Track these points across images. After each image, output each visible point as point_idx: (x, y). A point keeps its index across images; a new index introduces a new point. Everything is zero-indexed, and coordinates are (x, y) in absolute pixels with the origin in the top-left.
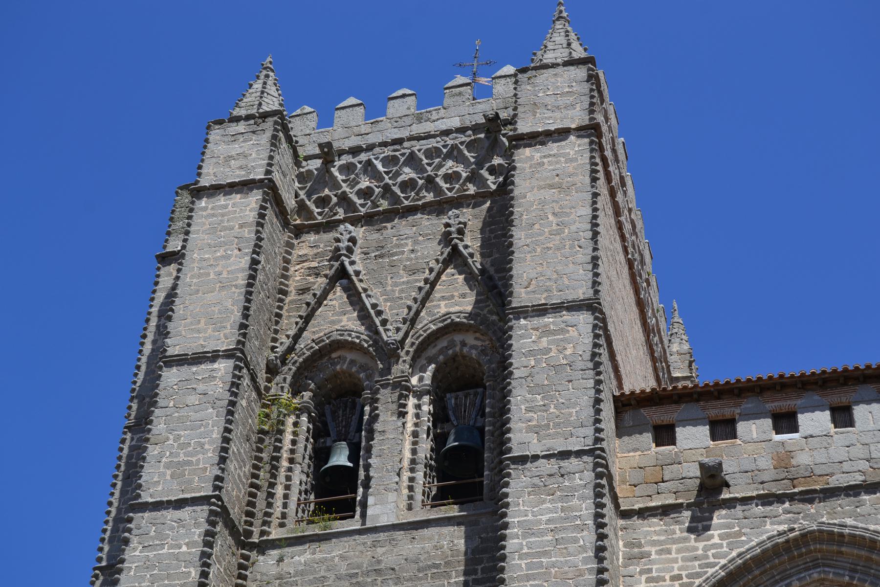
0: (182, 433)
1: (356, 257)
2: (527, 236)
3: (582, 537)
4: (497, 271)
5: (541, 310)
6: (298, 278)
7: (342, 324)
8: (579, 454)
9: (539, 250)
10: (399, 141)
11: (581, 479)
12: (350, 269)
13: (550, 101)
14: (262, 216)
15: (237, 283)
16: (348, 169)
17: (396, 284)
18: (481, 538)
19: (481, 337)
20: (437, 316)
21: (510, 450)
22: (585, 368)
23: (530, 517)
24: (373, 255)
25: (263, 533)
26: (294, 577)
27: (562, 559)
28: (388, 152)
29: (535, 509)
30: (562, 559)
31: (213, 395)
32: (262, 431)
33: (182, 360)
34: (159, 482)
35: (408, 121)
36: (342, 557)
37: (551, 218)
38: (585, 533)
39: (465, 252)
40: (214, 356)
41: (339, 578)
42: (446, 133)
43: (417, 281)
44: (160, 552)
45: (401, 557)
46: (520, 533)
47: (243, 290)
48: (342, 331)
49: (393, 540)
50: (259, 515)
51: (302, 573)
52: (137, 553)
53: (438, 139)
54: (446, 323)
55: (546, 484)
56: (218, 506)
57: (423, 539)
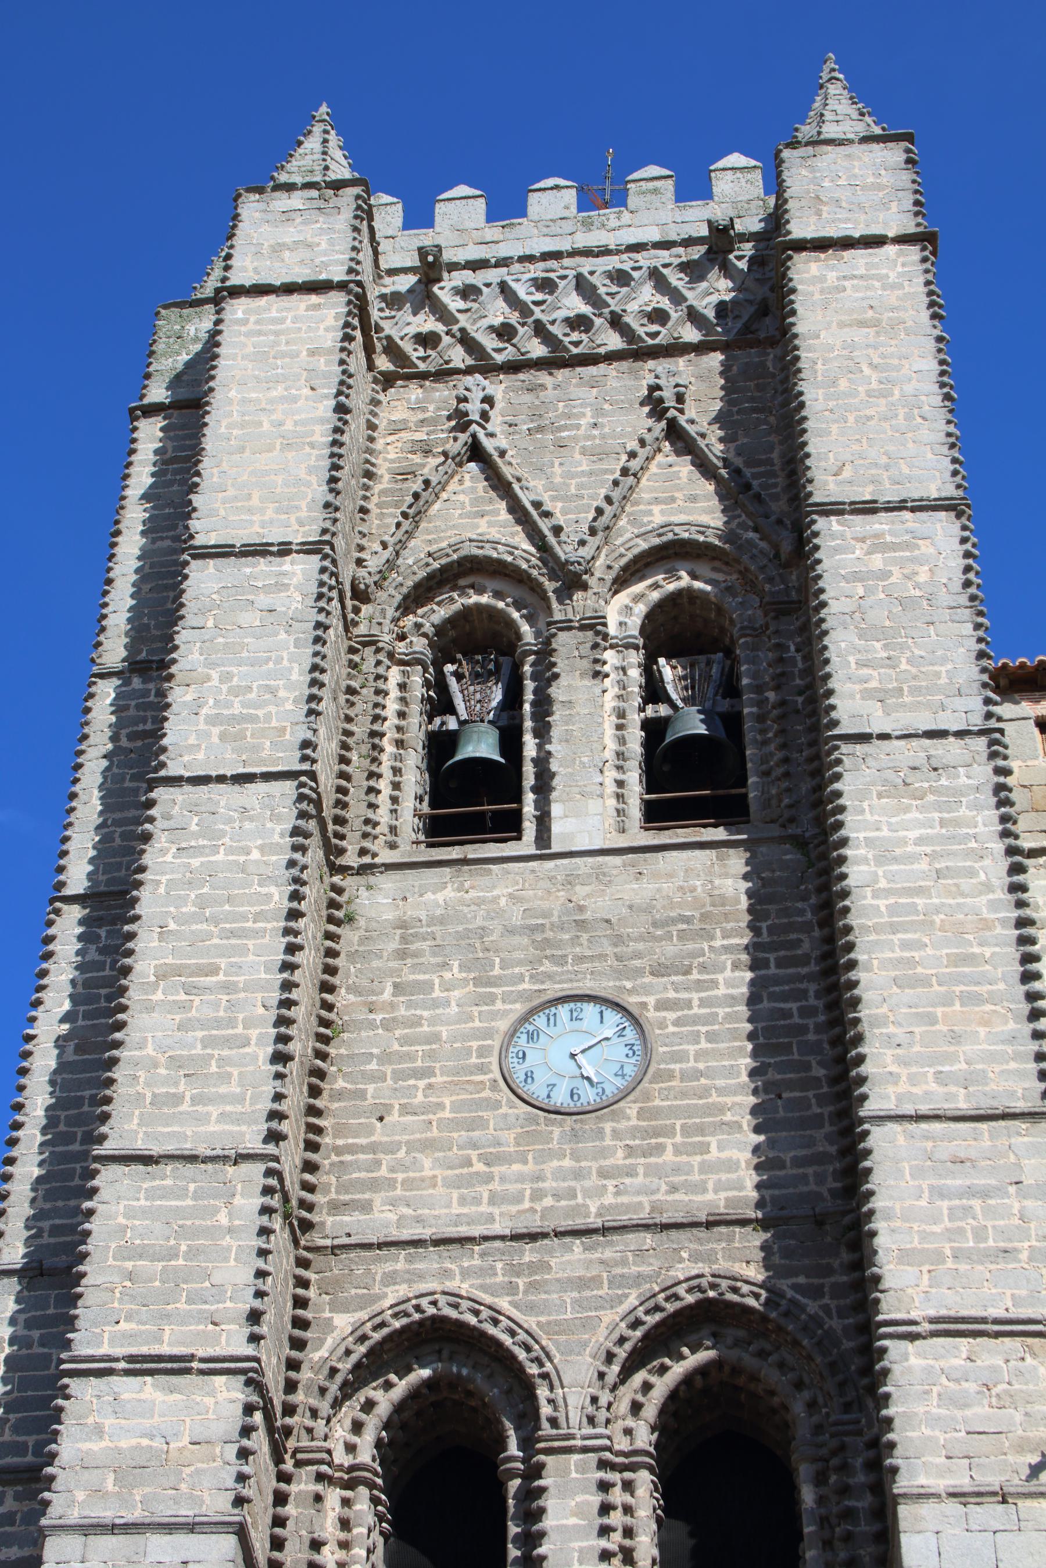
0: (234, 670)
1: (496, 423)
2: (828, 398)
3: (982, 868)
4: (748, 464)
5: (868, 508)
6: (392, 456)
7: (479, 531)
8: (960, 734)
9: (851, 419)
10: (557, 255)
11: (968, 777)
12: (488, 444)
13: (844, 195)
14: (348, 338)
15: (313, 439)
16: (467, 292)
17: (569, 475)
18: (762, 879)
19: (724, 568)
20: (649, 528)
21: (835, 723)
22: (954, 604)
23: (885, 833)
24: (525, 427)
25: (363, 852)
26: (428, 926)
27: (951, 901)
28: (537, 270)
29: (893, 820)
30: (951, 901)
31: (285, 613)
32: (351, 691)
33: (223, 552)
34: (199, 746)
35: (568, 226)
36: (511, 896)
37: (867, 371)
38: (987, 862)
39: (691, 429)
40: (284, 550)
41: (510, 931)
42: (637, 248)
43: (606, 471)
44: (212, 858)
45: (620, 902)
46: (870, 856)
47: (327, 451)
48: (480, 542)
49: (604, 875)
50: (357, 824)
51: (442, 921)
52: (169, 858)
53: (625, 257)
54: (664, 539)
55: (908, 781)
56: (311, 789)
57: (656, 876)
